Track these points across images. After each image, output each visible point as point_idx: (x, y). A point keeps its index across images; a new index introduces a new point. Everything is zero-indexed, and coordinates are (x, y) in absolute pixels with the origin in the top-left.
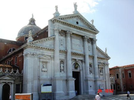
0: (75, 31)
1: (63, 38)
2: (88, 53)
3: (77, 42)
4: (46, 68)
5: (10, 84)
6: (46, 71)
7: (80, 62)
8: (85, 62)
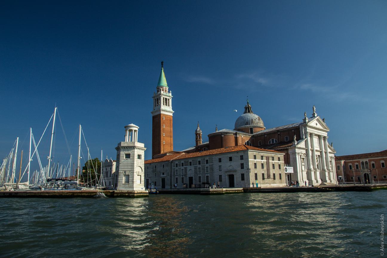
4: (304, 162)
6: (304, 165)
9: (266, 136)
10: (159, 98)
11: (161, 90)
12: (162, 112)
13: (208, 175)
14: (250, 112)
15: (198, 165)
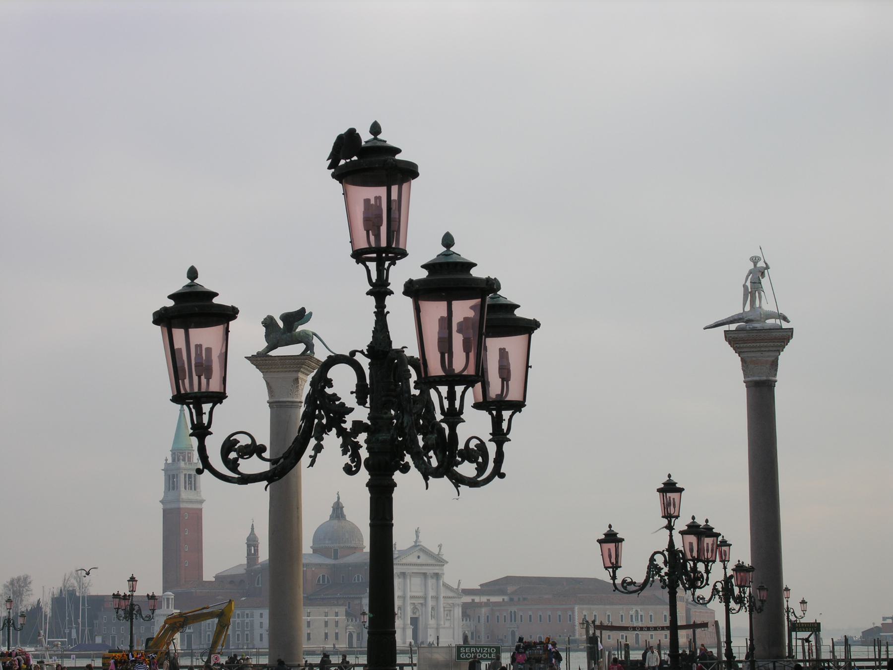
0: (415, 569)
1: (400, 580)
2: (431, 593)
3: (417, 581)
5: (353, 633)
7: (420, 605)
8: (425, 605)
9: (350, 568)
10: (177, 475)
11: (181, 461)
12: (183, 505)
13: (248, 632)
14: (339, 517)
15: (237, 619)
